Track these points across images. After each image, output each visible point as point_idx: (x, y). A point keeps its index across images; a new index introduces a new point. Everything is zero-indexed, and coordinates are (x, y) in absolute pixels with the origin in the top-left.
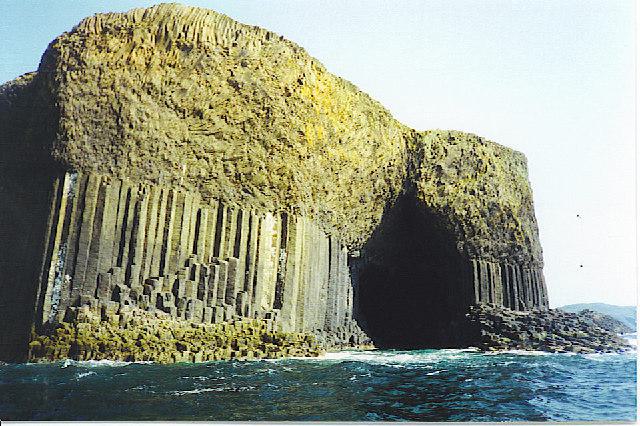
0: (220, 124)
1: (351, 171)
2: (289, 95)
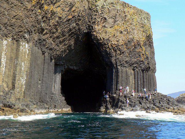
1: (57, 19)
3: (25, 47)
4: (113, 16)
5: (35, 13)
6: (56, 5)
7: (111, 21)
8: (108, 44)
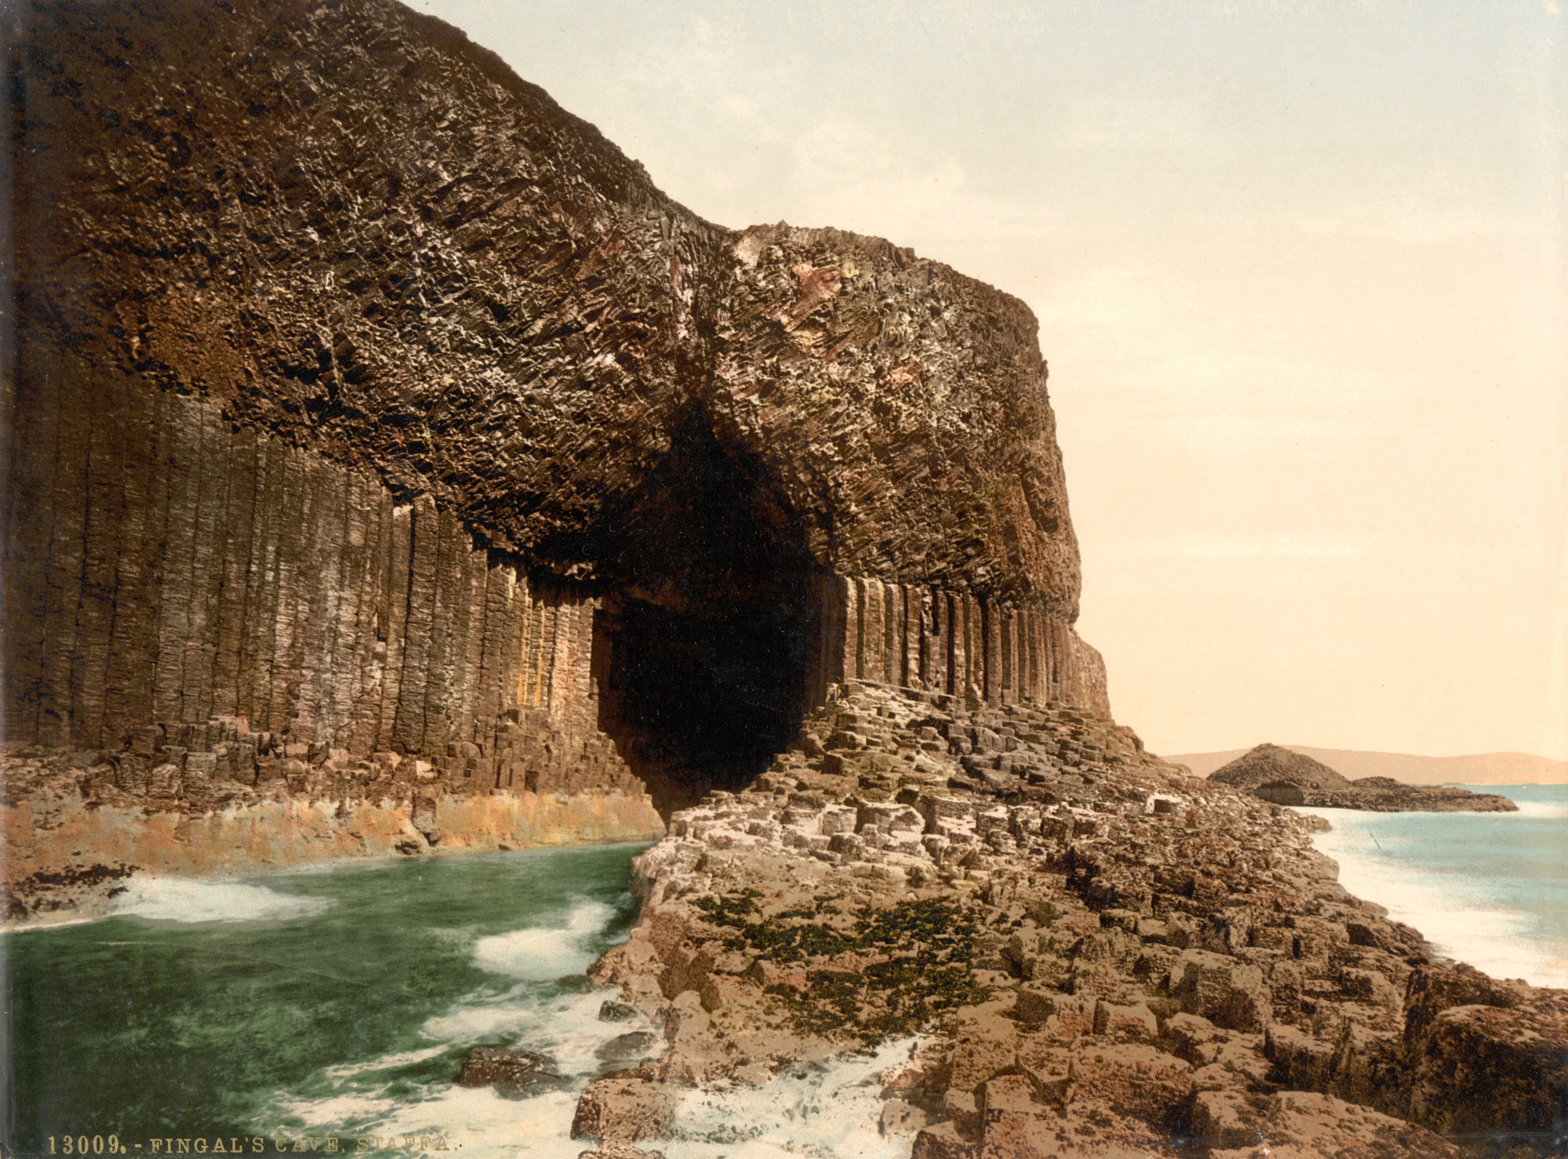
4: (817, 313)
8: (790, 457)
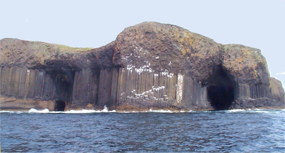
0: (159, 52)
2: (177, 41)
3: (181, 77)
5: (186, 59)
6: (198, 53)
7: (233, 57)
